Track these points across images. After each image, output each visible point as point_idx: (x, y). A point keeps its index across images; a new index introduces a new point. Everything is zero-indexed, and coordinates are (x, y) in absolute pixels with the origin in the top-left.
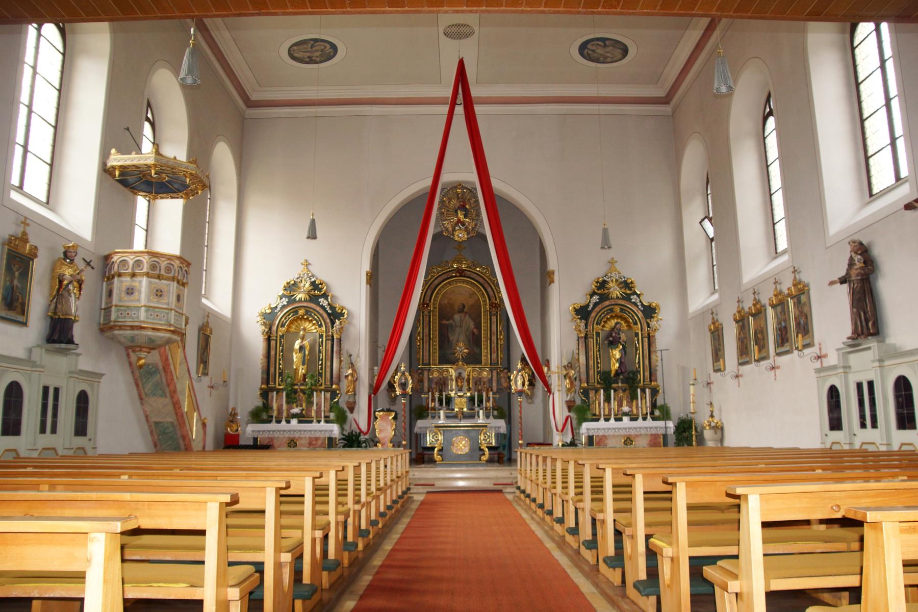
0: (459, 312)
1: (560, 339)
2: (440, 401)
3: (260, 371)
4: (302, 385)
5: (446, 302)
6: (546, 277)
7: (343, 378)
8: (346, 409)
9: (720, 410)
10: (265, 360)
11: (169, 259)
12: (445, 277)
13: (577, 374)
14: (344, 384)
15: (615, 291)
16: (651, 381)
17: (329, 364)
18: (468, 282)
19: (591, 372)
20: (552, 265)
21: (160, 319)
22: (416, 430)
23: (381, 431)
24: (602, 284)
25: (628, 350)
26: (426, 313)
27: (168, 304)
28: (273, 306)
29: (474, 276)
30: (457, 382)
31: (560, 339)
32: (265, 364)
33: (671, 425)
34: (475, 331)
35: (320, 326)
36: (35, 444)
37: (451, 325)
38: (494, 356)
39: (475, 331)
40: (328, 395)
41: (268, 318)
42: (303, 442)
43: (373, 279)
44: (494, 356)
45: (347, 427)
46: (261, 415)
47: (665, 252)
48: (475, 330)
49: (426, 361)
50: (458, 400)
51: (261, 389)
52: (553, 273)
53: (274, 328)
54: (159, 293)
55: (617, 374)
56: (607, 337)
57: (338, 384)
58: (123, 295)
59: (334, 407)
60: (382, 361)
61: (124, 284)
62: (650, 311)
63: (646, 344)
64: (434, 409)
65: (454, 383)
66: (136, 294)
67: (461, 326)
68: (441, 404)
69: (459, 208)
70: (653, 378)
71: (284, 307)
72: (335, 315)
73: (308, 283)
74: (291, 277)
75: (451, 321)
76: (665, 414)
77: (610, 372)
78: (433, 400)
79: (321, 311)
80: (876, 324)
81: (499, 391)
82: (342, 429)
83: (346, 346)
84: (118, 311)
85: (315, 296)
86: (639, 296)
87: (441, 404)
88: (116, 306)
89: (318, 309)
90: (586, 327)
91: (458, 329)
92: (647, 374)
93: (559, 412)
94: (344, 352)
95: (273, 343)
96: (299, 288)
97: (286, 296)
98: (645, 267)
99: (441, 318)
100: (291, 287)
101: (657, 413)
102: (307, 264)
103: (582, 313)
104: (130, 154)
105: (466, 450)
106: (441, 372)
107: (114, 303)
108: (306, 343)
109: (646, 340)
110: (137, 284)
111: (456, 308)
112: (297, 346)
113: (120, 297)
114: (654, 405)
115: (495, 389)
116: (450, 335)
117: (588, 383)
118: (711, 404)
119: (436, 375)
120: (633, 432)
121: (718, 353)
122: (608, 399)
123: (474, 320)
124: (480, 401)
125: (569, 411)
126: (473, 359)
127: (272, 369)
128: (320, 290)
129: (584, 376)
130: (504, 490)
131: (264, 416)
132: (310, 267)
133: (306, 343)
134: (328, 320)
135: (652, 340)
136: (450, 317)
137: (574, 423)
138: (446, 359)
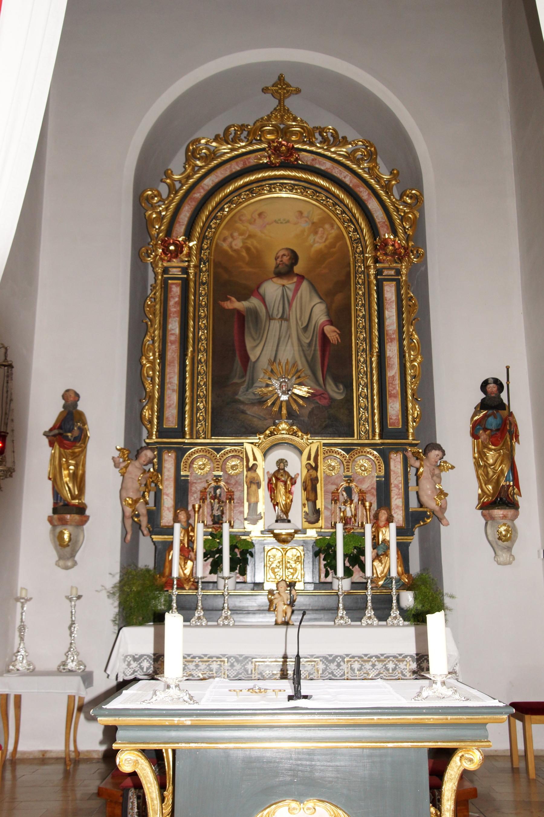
0: (279, 274)
2: (213, 554)
5: (238, 244)
12: (236, 167)
18: (304, 187)
26: (176, 272)
29: (326, 166)
30: (272, 489)
34: (332, 333)
37: (254, 313)
39: (332, 333)
44: (394, 408)
48: (329, 330)
64: (191, 581)
65: (263, 493)
67: (284, 318)
68: (216, 567)
75: (254, 302)
78: (187, 552)
87: (216, 567)
91: (275, 325)
111: (271, 263)
115: (399, 516)
116: (249, 344)
123: (326, 297)
124: (355, 559)
136: (251, 290)
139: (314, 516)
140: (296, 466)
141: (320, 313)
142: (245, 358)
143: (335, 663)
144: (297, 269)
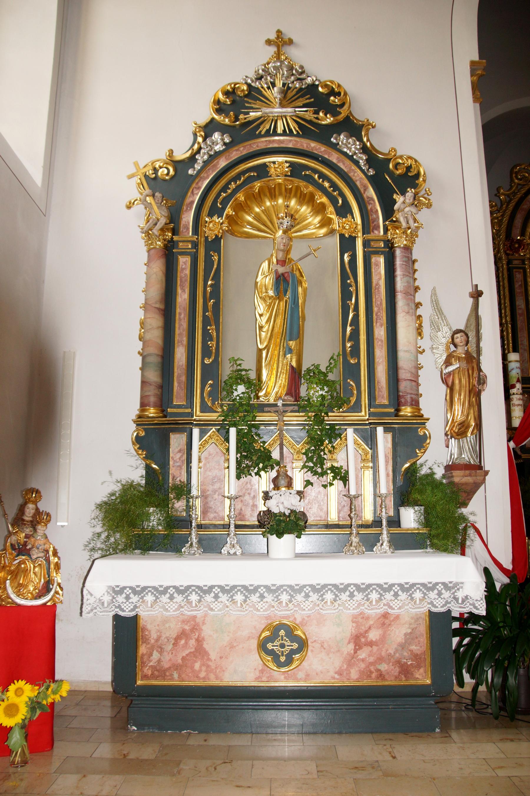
10: (156, 322)
17: (380, 332)
28: (181, 154)
32: (156, 335)
35: (344, 211)
51: (141, 420)
53: (188, 218)
71: (214, 157)
72: (394, 180)
74: (241, 71)
95: (184, 263)
97: (223, 129)
128: (333, 110)
131: (154, 520)
134: (371, 192)
143: (392, 593)
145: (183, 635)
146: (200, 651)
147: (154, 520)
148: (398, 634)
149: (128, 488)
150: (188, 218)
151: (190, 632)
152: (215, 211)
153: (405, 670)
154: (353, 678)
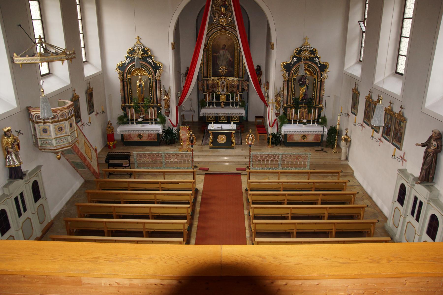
1: (275, 79)
3: (120, 96)
4: (142, 104)
5: (216, 43)
6: (269, 46)
7: (162, 100)
8: (164, 115)
9: (351, 132)
11: (62, 111)
13: (282, 99)
14: (163, 103)
15: (306, 54)
16: (319, 104)
17: (155, 93)
19: (289, 99)
20: (273, 40)
21: (64, 142)
22: (201, 114)
23: (183, 135)
24: (299, 52)
25: (309, 87)
27: (66, 133)
31: (275, 79)
32: (123, 94)
33: (326, 130)
36: (18, 227)
37: (218, 56)
38: (241, 73)
40: (156, 109)
41: (122, 68)
42: (145, 135)
43: (176, 46)
44: (241, 73)
45: (166, 125)
46: (124, 120)
47: (337, 33)
49: (205, 76)
50: (221, 97)
51: (122, 106)
52: (273, 44)
53: (125, 75)
54: (60, 129)
55: (302, 99)
56: (300, 80)
57: (161, 103)
58: (42, 133)
59: (159, 114)
60: (182, 93)
61: (41, 127)
62: (323, 67)
63: (319, 85)
66: (48, 132)
69: (222, 5)
70: (320, 103)
72: (156, 67)
73: (140, 51)
75: (218, 54)
76: (323, 122)
77: (299, 98)
79: (149, 66)
80: (433, 178)
81: (243, 90)
82: (164, 126)
83: (163, 83)
84: (41, 141)
85: (145, 57)
86: (318, 58)
88: (39, 138)
89: (147, 65)
90: (289, 76)
91: (222, 58)
92: (318, 100)
93: (271, 116)
94: (162, 86)
95: (125, 83)
96: (136, 53)
97: (129, 57)
98: (324, 43)
99: (213, 52)
100: (132, 52)
101: (320, 121)
102: (139, 38)
103: (288, 67)
104: (25, 57)
105: (225, 141)
106: (213, 81)
107: (38, 137)
108: (142, 82)
109: (319, 83)
110: (47, 127)
111: (221, 47)
112: (138, 84)
113: (40, 134)
114: (319, 116)
115: (240, 90)
117: (287, 104)
118: (347, 129)
119: (210, 82)
120: (306, 133)
121: (355, 105)
122: (296, 113)
125: (277, 117)
126: (230, 73)
127: (126, 96)
129: (285, 101)
130: (242, 173)
132: (141, 40)
133: (142, 82)
135: (322, 83)
137: (279, 124)
138: (216, 73)
139: (227, 91)
140: (225, 83)
141: (229, 56)
142: (217, 63)
144: (226, 48)
145: (129, 135)
146: (131, 137)
147: (125, 120)
148: (153, 135)
149: (121, 116)
150: (125, 75)
151: (130, 135)
152: (129, 74)
153: (154, 140)
154: (148, 140)
